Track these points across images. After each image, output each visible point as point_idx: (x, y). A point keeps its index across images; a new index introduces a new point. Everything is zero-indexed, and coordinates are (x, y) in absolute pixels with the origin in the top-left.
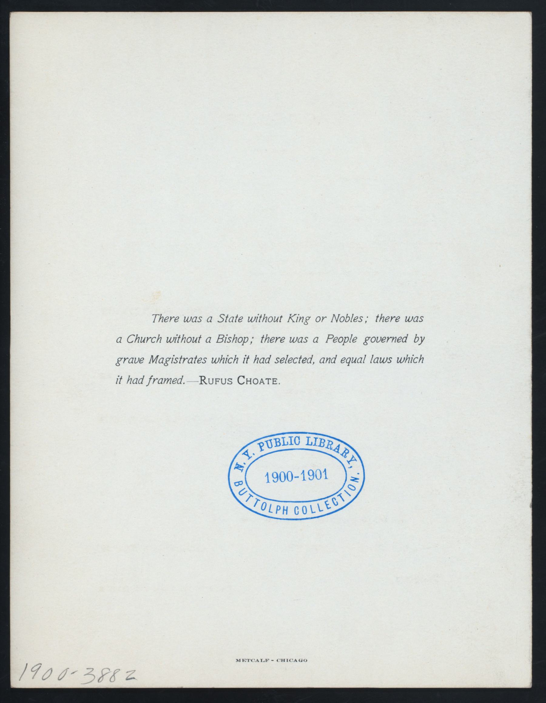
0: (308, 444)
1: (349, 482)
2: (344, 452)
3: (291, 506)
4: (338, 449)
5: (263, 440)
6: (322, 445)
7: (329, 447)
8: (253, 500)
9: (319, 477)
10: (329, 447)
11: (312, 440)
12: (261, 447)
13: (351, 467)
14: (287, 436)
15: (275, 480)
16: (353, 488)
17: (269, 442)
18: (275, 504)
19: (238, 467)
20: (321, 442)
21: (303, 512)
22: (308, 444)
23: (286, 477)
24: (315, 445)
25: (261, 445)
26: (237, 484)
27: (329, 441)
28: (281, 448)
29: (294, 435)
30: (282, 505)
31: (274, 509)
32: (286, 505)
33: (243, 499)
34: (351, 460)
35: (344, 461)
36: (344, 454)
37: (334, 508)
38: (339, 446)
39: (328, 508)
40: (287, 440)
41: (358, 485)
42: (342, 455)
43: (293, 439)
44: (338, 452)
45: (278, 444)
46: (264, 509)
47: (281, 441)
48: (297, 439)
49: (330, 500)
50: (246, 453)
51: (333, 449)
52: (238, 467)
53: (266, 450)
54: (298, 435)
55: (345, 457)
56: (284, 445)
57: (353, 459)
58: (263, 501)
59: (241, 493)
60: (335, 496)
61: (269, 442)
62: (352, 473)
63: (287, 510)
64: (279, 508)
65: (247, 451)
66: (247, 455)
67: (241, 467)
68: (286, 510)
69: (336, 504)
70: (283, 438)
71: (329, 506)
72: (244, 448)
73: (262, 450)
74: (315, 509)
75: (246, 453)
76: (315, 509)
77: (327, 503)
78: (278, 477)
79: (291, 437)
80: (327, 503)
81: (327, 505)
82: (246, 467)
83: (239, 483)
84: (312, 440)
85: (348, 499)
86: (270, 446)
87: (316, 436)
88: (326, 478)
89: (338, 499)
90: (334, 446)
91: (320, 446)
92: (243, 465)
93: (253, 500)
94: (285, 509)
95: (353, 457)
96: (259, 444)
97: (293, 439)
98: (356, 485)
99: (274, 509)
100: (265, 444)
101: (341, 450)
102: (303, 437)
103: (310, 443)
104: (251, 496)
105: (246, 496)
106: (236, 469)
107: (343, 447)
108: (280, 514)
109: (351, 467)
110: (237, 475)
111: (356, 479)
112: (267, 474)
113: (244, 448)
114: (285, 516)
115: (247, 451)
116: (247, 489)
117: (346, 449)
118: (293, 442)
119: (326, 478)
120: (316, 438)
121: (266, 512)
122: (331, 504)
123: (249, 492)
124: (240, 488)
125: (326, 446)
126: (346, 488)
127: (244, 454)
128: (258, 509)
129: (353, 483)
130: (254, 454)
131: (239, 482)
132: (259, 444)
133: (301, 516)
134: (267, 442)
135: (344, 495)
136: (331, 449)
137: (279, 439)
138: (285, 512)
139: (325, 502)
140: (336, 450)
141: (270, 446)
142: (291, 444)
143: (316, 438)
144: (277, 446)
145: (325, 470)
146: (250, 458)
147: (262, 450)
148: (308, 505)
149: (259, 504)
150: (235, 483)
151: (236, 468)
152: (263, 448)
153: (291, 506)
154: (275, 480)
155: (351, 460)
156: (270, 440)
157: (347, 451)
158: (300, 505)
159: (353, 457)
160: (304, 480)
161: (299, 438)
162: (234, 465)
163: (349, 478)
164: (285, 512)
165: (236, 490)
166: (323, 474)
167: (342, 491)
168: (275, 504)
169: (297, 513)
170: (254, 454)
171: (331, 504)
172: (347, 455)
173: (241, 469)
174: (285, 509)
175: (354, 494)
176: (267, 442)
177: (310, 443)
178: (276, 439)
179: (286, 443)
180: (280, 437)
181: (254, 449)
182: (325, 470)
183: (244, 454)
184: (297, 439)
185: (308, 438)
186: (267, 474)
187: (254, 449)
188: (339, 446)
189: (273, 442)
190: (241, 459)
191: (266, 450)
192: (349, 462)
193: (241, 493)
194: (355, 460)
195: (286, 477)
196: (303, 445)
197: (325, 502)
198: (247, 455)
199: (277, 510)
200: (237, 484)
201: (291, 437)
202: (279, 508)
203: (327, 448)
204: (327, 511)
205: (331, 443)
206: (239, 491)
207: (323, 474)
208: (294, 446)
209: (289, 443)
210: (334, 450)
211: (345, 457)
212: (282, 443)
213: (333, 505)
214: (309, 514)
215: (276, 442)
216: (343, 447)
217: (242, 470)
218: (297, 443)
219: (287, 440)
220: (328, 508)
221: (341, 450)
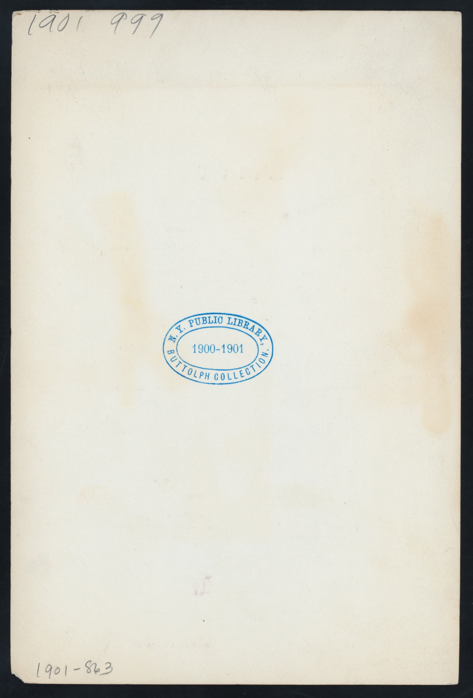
0: (229, 324)
1: (260, 356)
3: (212, 373)
4: (253, 329)
5: (193, 318)
6: (240, 324)
7: (246, 326)
8: (181, 366)
9: (236, 351)
10: (246, 326)
11: (232, 320)
12: (191, 323)
13: (263, 344)
14: (212, 316)
17: (198, 320)
18: (199, 371)
19: (172, 338)
22: (229, 324)
23: (209, 348)
24: (235, 324)
26: (170, 352)
27: (246, 322)
28: (208, 325)
29: (218, 316)
30: (205, 371)
31: (198, 375)
32: (208, 371)
33: (174, 364)
34: (263, 338)
35: (257, 338)
36: (258, 334)
37: (247, 377)
38: (254, 326)
39: (242, 377)
40: (212, 319)
41: (267, 359)
42: (256, 334)
44: (252, 331)
47: (208, 320)
48: (220, 319)
49: (244, 370)
51: (249, 328)
52: (172, 338)
54: (221, 315)
56: (210, 323)
58: (189, 367)
59: (172, 360)
60: (248, 367)
61: (198, 320)
62: (263, 349)
66: (180, 330)
67: (175, 338)
68: (208, 376)
69: (248, 373)
70: (209, 317)
72: (177, 323)
74: (232, 376)
76: (232, 376)
77: (241, 372)
78: (203, 348)
79: (215, 317)
80: (241, 372)
81: (241, 374)
82: (178, 339)
83: (171, 352)
84: (232, 320)
85: (258, 370)
86: (198, 323)
88: (242, 352)
89: (251, 369)
90: (250, 327)
91: (238, 325)
92: (175, 337)
93: (181, 366)
94: (207, 375)
95: (265, 336)
96: (190, 321)
97: (217, 318)
98: (266, 359)
99: (198, 375)
100: (194, 321)
101: (256, 330)
103: (230, 323)
104: (180, 362)
105: (176, 362)
109: (263, 344)
110: (170, 345)
113: (177, 323)
114: (207, 381)
115: (179, 326)
116: (177, 357)
117: (259, 329)
118: (217, 321)
119: (242, 352)
120: (235, 319)
121: (191, 377)
123: (179, 359)
124: (172, 355)
125: (243, 325)
126: (257, 361)
127: (177, 328)
129: (263, 357)
131: (171, 351)
132: (190, 321)
133: (220, 381)
134: (196, 319)
135: (256, 367)
136: (247, 328)
137: (206, 318)
138: (207, 377)
139: (240, 371)
140: (252, 330)
142: (215, 322)
143: (235, 319)
144: (204, 323)
145: (241, 345)
146: (181, 332)
147: (192, 326)
148: (225, 373)
149: (187, 369)
150: (168, 352)
152: (192, 324)
155: (263, 338)
156: (199, 319)
158: (220, 373)
159: (265, 336)
160: (224, 352)
161: (222, 318)
163: (260, 353)
166: (240, 349)
168: (199, 371)
173: (174, 340)
174: (207, 375)
175: (263, 366)
176: (196, 319)
177: (230, 323)
178: (203, 318)
179: (211, 322)
180: (207, 316)
181: (185, 325)
182: (241, 345)
183: (177, 328)
184: (220, 319)
185: (230, 318)
187: (185, 325)
188: (254, 326)
189: (201, 320)
190: (175, 333)
192: (261, 340)
193: (172, 360)
195: (209, 348)
196: (225, 323)
197: (240, 371)
198: (180, 330)
199: (201, 375)
200: (170, 352)
202: (202, 374)
203: (244, 327)
204: (240, 379)
206: (172, 358)
208: (218, 325)
209: (214, 322)
210: (250, 330)
211: (258, 335)
212: (208, 322)
214: (226, 381)
215: (204, 320)
217: (174, 342)
218: (220, 321)
219: (212, 319)
220: (242, 377)
221: (256, 330)
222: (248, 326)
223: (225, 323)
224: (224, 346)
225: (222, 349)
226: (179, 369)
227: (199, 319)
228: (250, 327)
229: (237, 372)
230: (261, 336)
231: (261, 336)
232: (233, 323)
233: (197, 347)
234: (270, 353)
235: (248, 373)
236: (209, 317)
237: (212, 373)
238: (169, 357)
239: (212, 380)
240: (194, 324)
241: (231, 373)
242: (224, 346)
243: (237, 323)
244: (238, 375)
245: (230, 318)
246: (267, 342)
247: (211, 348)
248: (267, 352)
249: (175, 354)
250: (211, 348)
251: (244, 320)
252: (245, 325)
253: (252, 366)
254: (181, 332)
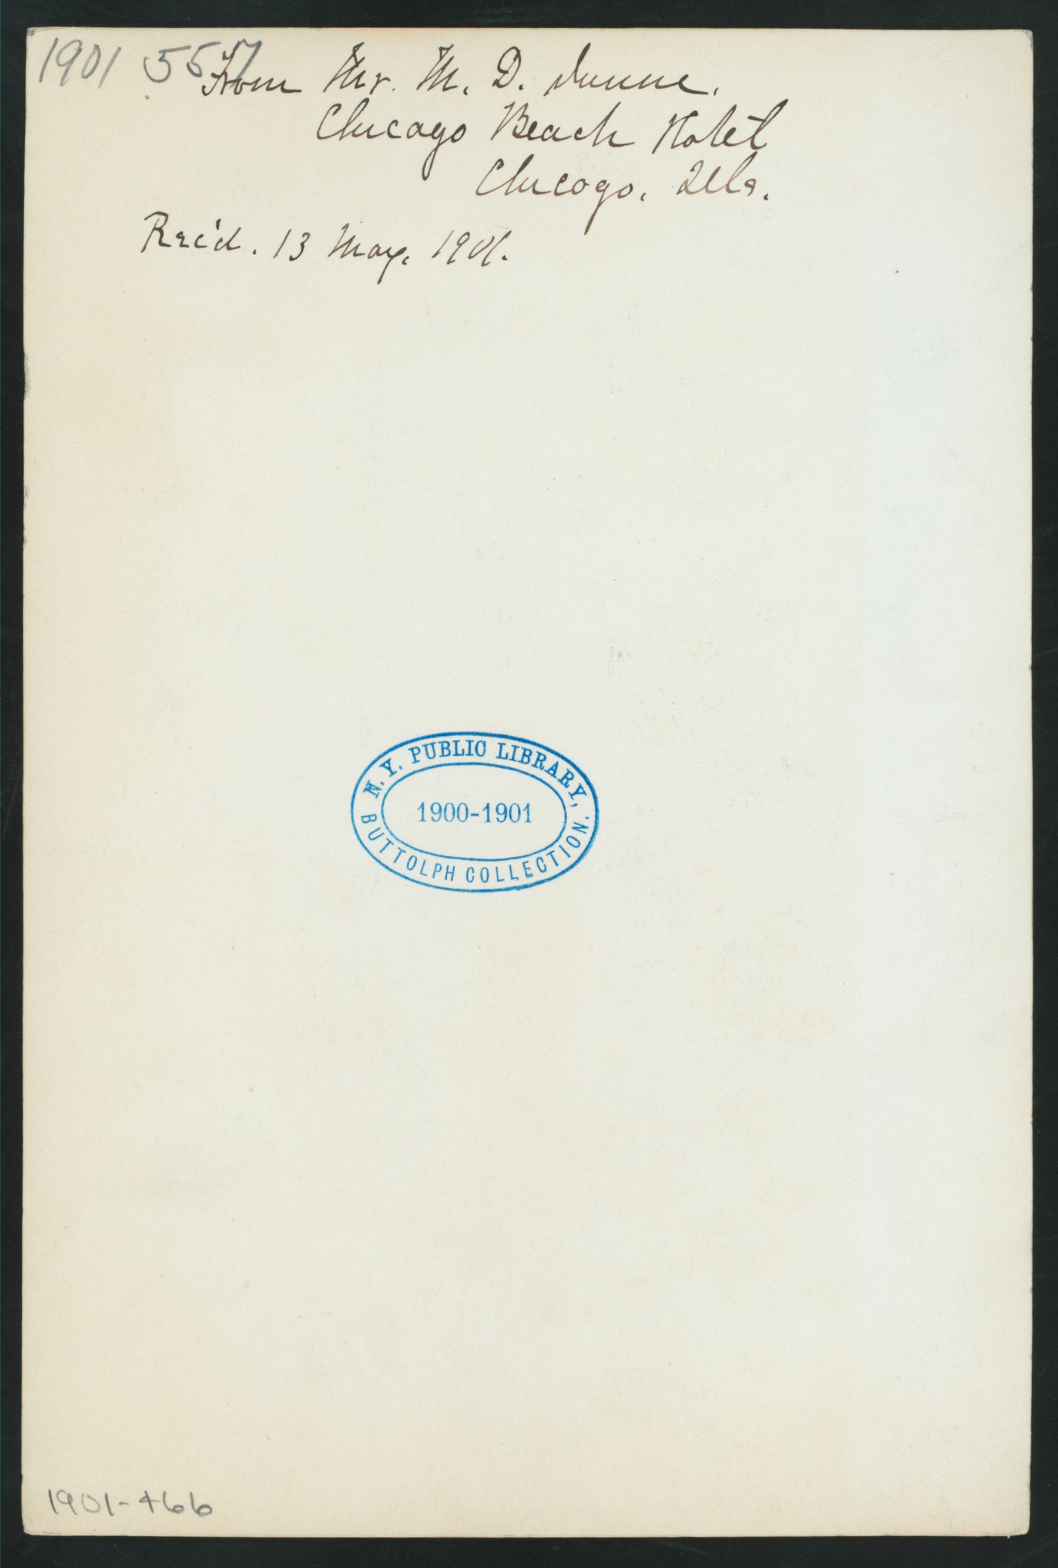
1: (569, 831)
2: (565, 777)
4: (555, 772)
8: (392, 851)
11: (508, 749)
12: (414, 755)
13: (575, 805)
14: (463, 739)
15: (436, 817)
16: (576, 844)
17: (430, 748)
19: (369, 788)
20: (524, 755)
21: (484, 880)
22: (500, 757)
23: (456, 812)
24: (513, 759)
25: (416, 751)
26: (366, 819)
27: (540, 754)
29: (477, 739)
31: (429, 869)
32: (451, 863)
33: (375, 846)
34: (577, 792)
36: (565, 781)
37: (538, 876)
38: (556, 764)
40: (463, 745)
41: (584, 839)
42: (561, 781)
43: (473, 745)
44: (554, 775)
45: (446, 752)
46: (411, 865)
48: (481, 745)
49: (532, 861)
50: (387, 765)
51: (547, 767)
52: (369, 788)
53: (424, 761)
55: (566, 785)
56: (457, 754)
57: (581, 791)
58: (410, 852)
59: (372, 836)
60: (543, 855)
61: (430, 748)
63: (453, 873)
64: (438, 868)
65: (388, 761)
66: (389, 768)
67: (377, 789)
68: (450, 873)
69: (543, 868)
71: (529, 872)
72: (385, 753)
73: (416, 761)
74: (504, 873)
75: (387, 765)
76: (504, 873)
77: (527, 865)
79: (470, 742)
80: (527, 865)
83: (368, 819)
84: (508, 749)
85: (564, 862)
86: (431, 755)
87: (516, 743)
88: (528, 821)
89: (548, 860)
90: (547, 765)
91: (522, 761)
92: (380, 786)
93: (392, 851)
94: (450, 870)
95: (580, 787)
96: (412, 749)
97: (473, 745)
100: (423, 749)
101: (560, 773)
102: (493, 744)
103: (503, 755)
105: (382, 842)
106: (367, 793)
107: (563, 768)
108: (440, 880)
109: (575, 805)
110: (367, 803)
111: (583, 827)
112: (422, 806)
115: (388, 761)
116: (383, 829)
117: (569, 772)
118: (473, 751)
119: (528, 821)
120: (515, 747)
121: (415, 874)
122: (534, 870)
123: (387, 835)
124: (372, 826)
126: (562, 841)
127: (383, 765)
128: (401, 867)
129: (576, 834)
130: (401, 768)
132: (412, 749)
133: (478, 884)
134: (426, 746)
135: (559, 855)
136: (541, 768)
137: (449, 744)
138: (449, 876)
140: (552, 772)
141: (431, 755)
142: (469, 754)
143: (515, 747)
144: (443, 755)
145: (528, 806)
146: (393, 773)
147: (416, 761)
149: (404, 858)
151: (366, 789)
152: (417, 757)
153: (461, 867)
154: (436, 817)
155: (577, 792)
156: (432, 744)
157: (569, 776)
158: (478, 866)
159: (580, 787)
160: (488, 820)
162: (363, 785)
163: (570, 824)
164: (449, 876)
165: (364, 830)
166: (524, 814)
167: (556, 847)
168: (432, 861)
169: (470, 878)
170: (401, 768)
171: (534, 870)
172: (570, 782)
173: (376, 792)
174: (450, 870)
175: (575, 853)
176: (426, 746)
177: (503, 755)
178: (442, 743)
179: (460, 752)
180: (450, 739)
181: (401, 758)
182: (528, 806)
183: (383, 765)
184: (481, 745)
185: (501, 745)
186: (422, 806)
187: (401, 758)
188: (556, 764)
190: (377, 775)
191: (424, 761)
192: (572, 795)
193: (372, 836)
194: (584, 793)
195: (456, 812)
196: (491, 756)
198: (389, 768)
200: (366, 819)
201: (470, 742)
203: (535, 766)
205: (542, 758)
206: (370, 832)
207: (524, 814)
208: (475, 759)
209: (466, 752)
210: (548, 772)
211: (566, 785)
212: (453, 752)
213: (537, 873)
214: (492, 884)
215: (443, 749)
216: (563, 768)
218: (481, 752)
219: (463, 745)
221: (560, 773)
222: (544, 763)
223: (491, 756)
224: (488, 807)
225: (483, 815)
226: (388, 857)
227: (432, 744)
228: (547, 765)
229: (517, 865)
230: (573, 786)
231: (573, 786)
232: (510, 756)
233: (427, 808)
234: (590, 824)
235: (543, 868)
236: (456, 742)
237: (461, 867)
238: (364, 830)
239: (460, 881)
240: (422, 756)
241: (503, 866)
242: (488, 807)
243: (518, 757)
244: (518, 870)
245: (501, 745)
246: (585, 802)
247: (458, 812)
248: (585, 823)
249: (379, 823)
250: (458, 812)
251: (535, 749)
252: (538, 759)
253: (551, 853)
254: (393, 773)
